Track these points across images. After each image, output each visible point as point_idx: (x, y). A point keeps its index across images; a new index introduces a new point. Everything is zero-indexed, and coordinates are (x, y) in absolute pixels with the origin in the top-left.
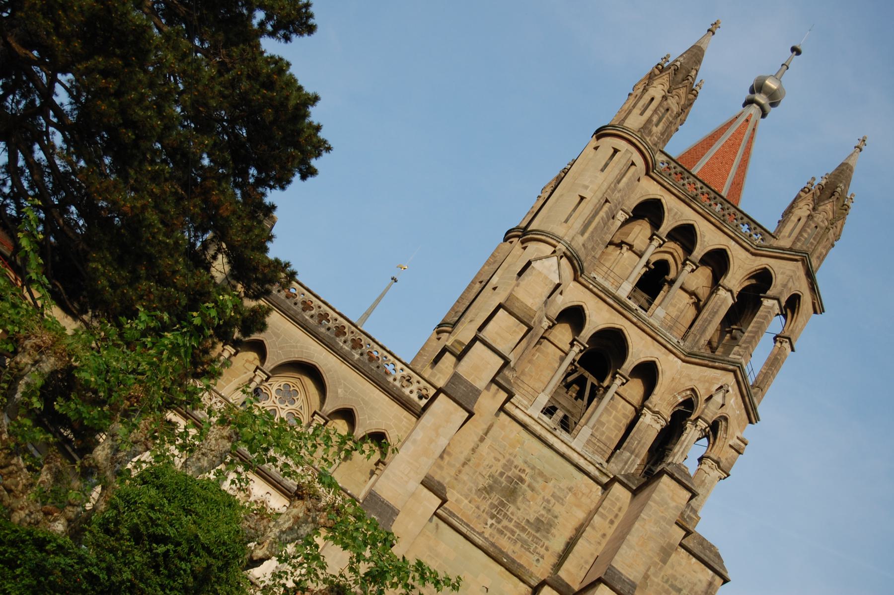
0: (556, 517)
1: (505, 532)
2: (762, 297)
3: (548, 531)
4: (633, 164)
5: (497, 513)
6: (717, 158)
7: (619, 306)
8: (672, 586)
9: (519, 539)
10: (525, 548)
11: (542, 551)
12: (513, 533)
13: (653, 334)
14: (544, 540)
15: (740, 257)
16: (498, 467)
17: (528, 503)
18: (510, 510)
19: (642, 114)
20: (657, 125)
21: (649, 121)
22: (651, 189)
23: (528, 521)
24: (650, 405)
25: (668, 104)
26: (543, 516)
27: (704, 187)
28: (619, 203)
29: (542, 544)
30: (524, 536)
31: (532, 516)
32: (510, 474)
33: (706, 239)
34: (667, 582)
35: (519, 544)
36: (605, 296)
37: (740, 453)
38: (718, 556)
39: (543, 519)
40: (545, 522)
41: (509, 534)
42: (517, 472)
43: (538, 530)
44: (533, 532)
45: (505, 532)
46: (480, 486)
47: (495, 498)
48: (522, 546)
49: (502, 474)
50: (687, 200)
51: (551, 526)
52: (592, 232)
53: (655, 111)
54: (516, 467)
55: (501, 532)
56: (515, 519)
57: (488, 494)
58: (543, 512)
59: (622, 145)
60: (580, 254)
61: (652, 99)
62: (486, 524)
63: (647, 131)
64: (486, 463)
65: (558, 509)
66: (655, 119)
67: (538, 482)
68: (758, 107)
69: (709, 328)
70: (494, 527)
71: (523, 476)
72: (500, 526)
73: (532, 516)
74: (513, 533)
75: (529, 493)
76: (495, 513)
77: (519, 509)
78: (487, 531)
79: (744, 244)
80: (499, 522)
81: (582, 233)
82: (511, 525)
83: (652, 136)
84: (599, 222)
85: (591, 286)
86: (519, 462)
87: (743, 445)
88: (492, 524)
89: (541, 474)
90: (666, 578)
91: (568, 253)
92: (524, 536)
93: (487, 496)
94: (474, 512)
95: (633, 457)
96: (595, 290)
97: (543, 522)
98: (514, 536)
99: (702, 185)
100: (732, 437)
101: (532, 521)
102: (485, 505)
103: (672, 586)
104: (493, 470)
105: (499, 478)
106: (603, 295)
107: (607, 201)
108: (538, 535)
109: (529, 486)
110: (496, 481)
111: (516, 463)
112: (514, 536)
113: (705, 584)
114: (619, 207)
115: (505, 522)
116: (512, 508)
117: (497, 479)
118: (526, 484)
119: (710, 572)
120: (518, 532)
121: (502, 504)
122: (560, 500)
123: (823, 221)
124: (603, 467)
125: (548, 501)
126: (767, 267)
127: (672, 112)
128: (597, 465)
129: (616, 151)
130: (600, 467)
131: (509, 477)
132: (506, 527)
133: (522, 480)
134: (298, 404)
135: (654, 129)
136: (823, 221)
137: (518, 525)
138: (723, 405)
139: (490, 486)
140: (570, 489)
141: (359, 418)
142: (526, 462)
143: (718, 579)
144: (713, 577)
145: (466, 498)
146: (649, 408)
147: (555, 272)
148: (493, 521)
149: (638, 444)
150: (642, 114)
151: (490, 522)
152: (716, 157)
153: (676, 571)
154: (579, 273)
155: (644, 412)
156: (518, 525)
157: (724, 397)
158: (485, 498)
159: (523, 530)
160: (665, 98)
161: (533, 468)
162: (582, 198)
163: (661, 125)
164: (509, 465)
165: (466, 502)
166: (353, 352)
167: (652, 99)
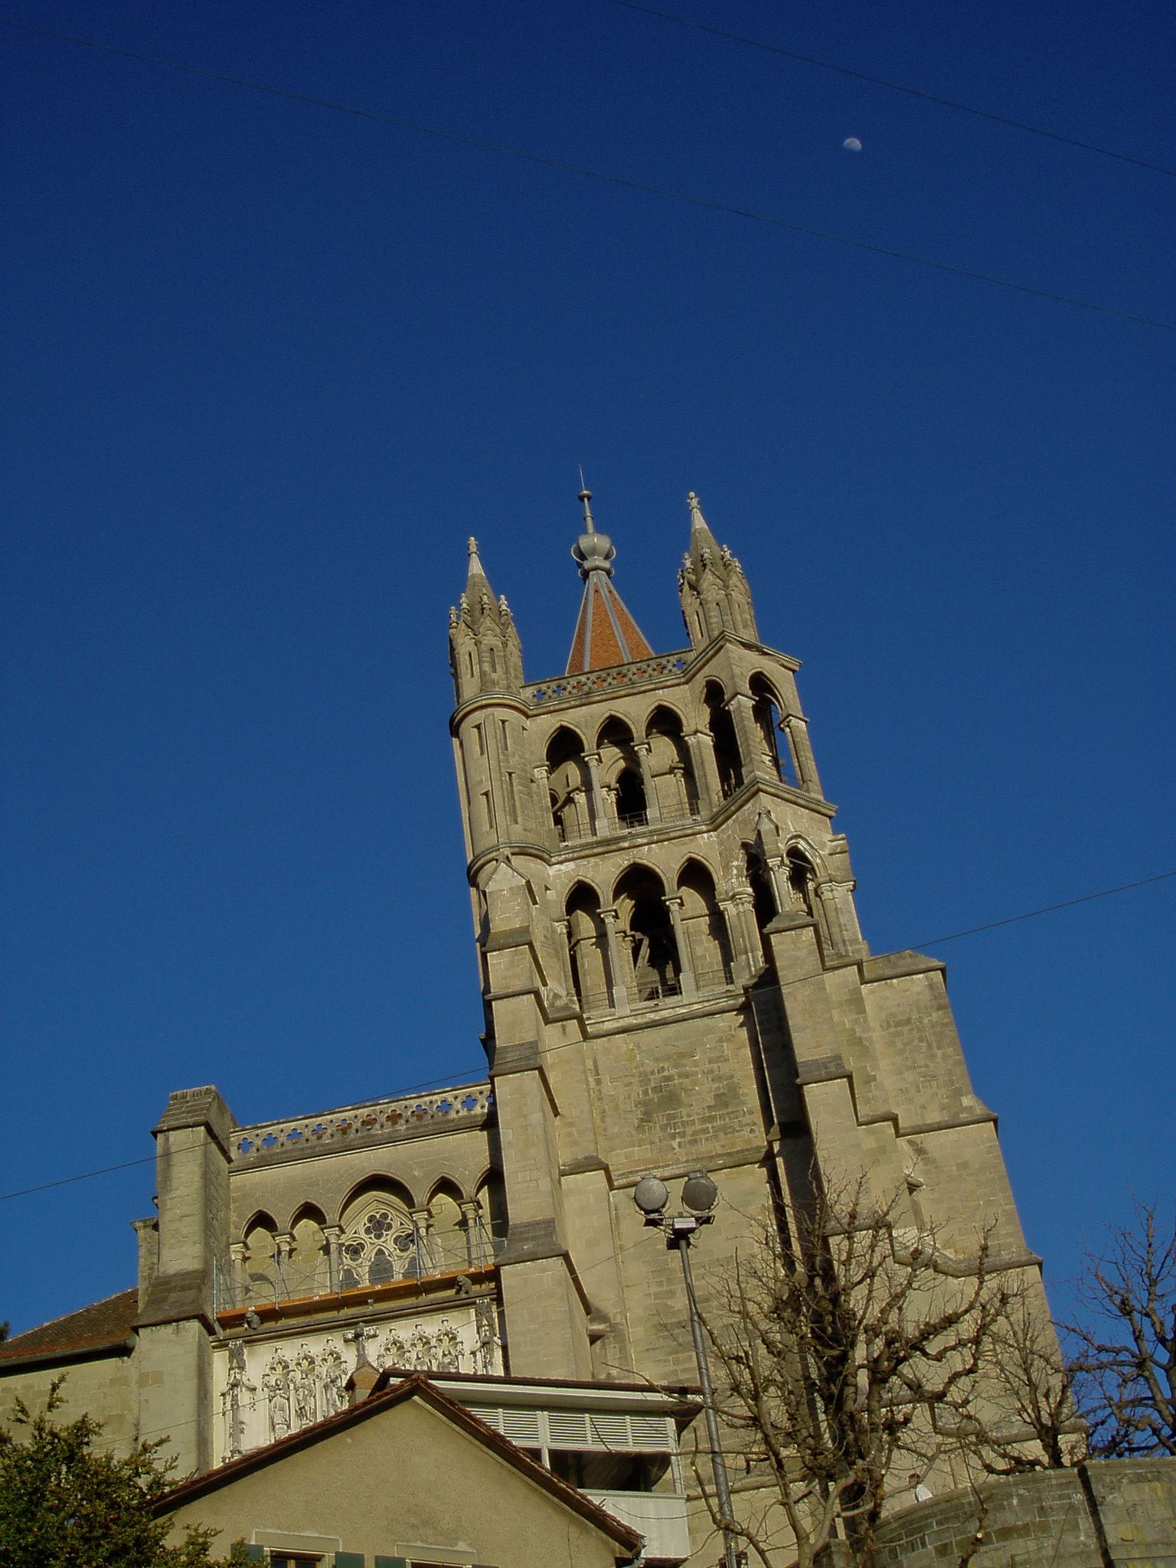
0: (732, 1076)
2: (724, 706)
3: (736, 1096)
4: (503, 722)
5: (675, 1129)
6: (597, 646)
8: (898, 1024)
9: (716, 1130)
11: (747, 1119)
12: (705, 1131)
14: (740, 1109)
16: (637, 1090)
17: (694, 1092)
18: (684, 1113)
21: (483, 674)
22: (546, 726)
24: (722, 897)
25: (485, 645)
26: (718, 1088)
28: (525, 765)
29: (742, 1112)
31: (709, 1099)
32: (653, 1085)
33: (633, 715)
34: (889, 1026)
39: (722, 1091)
40: (726, 1092)
41: (703, 1137)
43: (726, 1105)
47: (660, 1118)
48: (725, 1134)
49: (646, 1093)
50: (584, 701)
51: (735, 1089)
53: (480, 662)
54: (652, 1073)
55: (694, 1142)
57: (650, 1122)
58: (716, 1085)
59: (478, 717)
60: (530, 841)
62: (674, 1149)
63: (489, 684)
64: (621, 1098)
65: (725, 1069)
66: (487, 667)
67: (685, 1065)
68: (595, 572)
69: (709, 780)
70: (683, 1144)
71: (666, 1073)
73: (709, 1099)
74: (705, 1131)
76: (673, 1131)
77: (692, 1105)
79: (669, 683)
80: (683, 1135)
81: (516, 822)
82: (698, 1127)
83: (498, 684)
84: (520, 797)
86: (650, 1065)
89: (681, 1055)
90: (885, 1025)
93: (651, 1124)
95: (750, 954)
97: (724, 1094)
98: (709, 1133)
99: (585, 676)
101: (712, 1103)
102: (658, 1133)
103: (898, 1024)
104: (634, 1095)
105: (647, 1098)
106: (587, 852)
107: (510, 774)
109: (680, 1076)
110: (645, 1104)
111: (649, 1070)
112: (709, 1133)
114: (528, 768)
115: (689, 1130)
116: (684, 1111)
117: (645, 1101)
121: (670, 1117)
122: (722, 1059)
123: (718, 594)
124: (732, 991)
125: (711, 1071)
126: (707, 678)
127: (497, 646)
129: (478, 727)
130: (730, 994)
131: (654, 1089)
132: (695, 1133)
133: (668, 1079)
134: (396, 1224)
135: (494, 676)
136: (718, 594)
137: (704, 1120)
138: (777, 827)
139: (645, 1113)
140: (721, 1040)
141: (455, 1178)
142: (657, 1060)
145: (634, 1146)
146: (724, 900)
147: (513, 876)
148: (678, 1140)
149: (744, 940)
151: (675, 1144)
152: (595, 645)
153: (887, 1008)
154: (547, 857)
156: (704, 1120)
157: (771, 820)
158: (650, 1129)
159: (712, 1119)
161: (669, 1058)
162: (486, 794)
164: (644, 1078)
166: (397, 1127)
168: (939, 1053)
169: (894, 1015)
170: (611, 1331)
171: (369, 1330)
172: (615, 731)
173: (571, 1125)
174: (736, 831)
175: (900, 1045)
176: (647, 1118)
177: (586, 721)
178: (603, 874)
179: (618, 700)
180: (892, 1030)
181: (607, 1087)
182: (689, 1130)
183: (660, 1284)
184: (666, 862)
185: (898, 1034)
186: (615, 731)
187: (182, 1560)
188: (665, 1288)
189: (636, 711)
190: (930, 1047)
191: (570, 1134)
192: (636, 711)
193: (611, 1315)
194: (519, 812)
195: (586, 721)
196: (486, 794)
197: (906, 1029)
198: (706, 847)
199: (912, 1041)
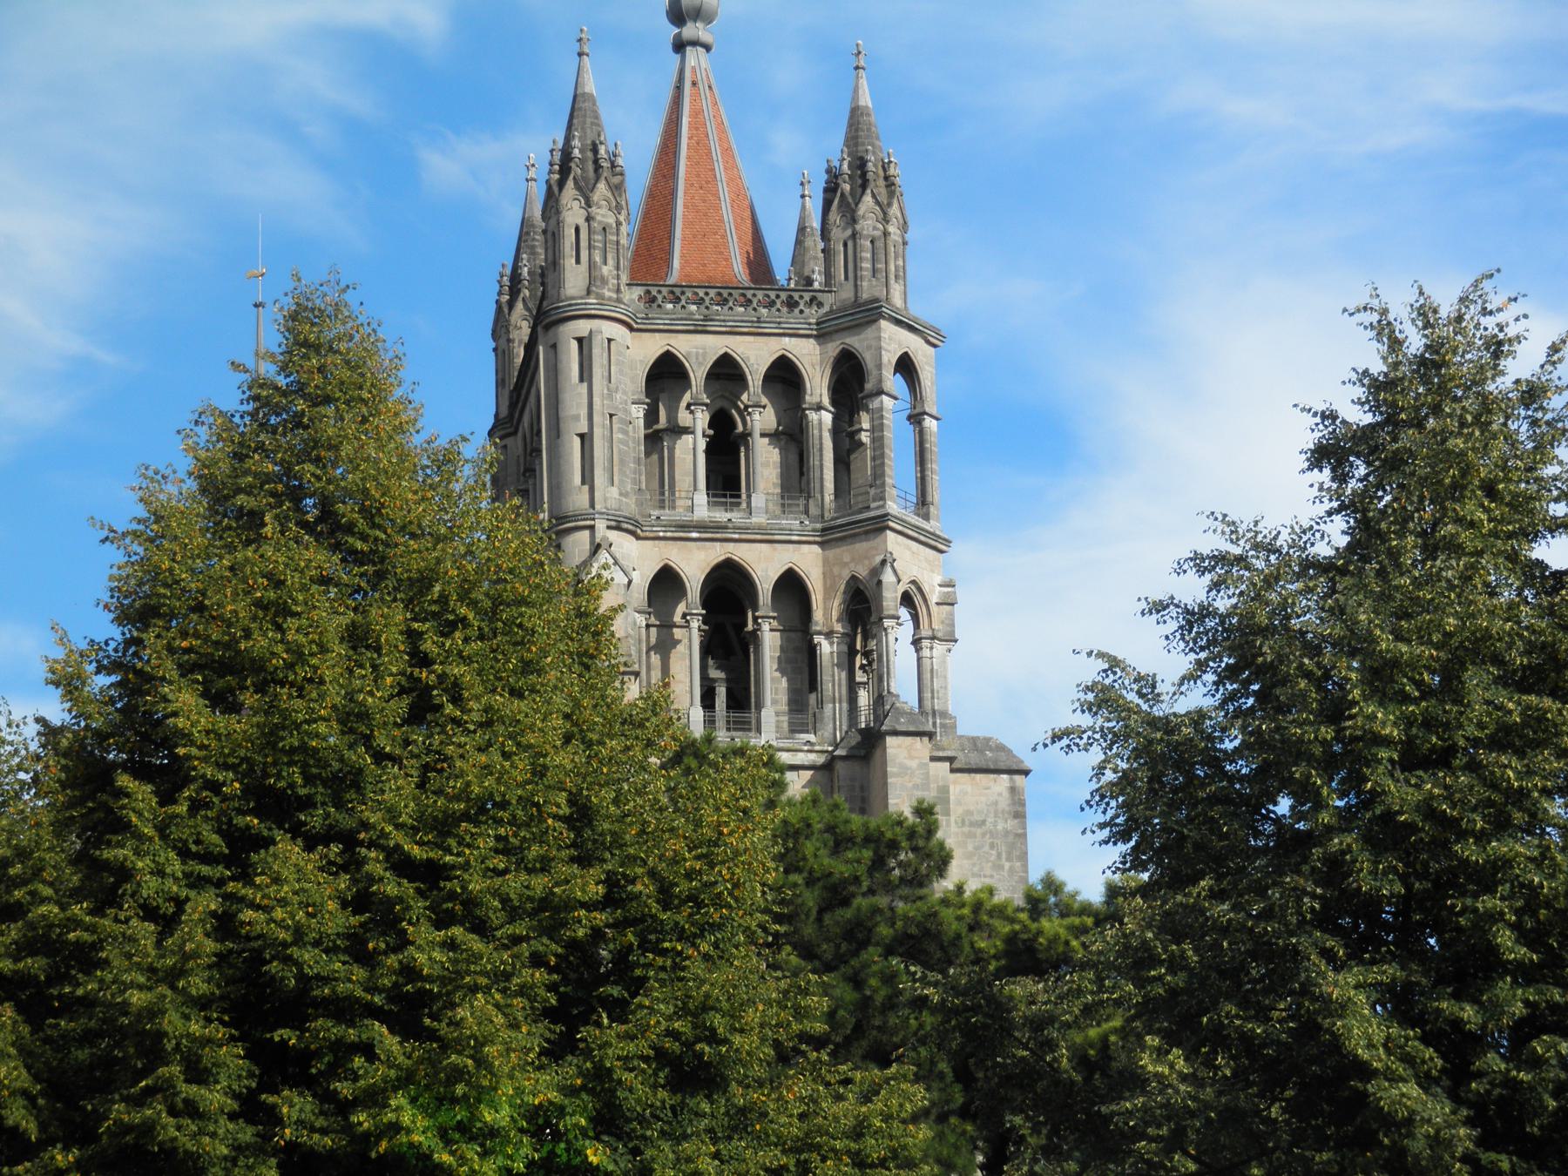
4: (610, 340)
7: (710, 531)
8: (972, 824)
13: (767, 537)
15: (804, 352)
19: (578, 261)
20: (605, 263)
21: (591, 265)
22: (648, 349)
25: (600, 222)
27: (708, 290)
34: (963, 822)
36: (684, 530)
37: (952, 604)
38: (1001, 748)
52: (620, 470)
59: (582, 327)
61: (577, 230)
63: (598, 283)
66: (598, 258)
79: (802, 332)
85: (661, 534)
87: (950, 589)
90: (960, 821)
91: (613, 523)
96: (669, 534)
100: (933, 591)
103: (972, 824)
107: (611, 416)
113: (1006, 794)
119: (1005, 776)
127: (611, 227)
128: (806, 748)
129: (580, 340)
143: (1017, 778)
144: (1011, 779)
146: (819, 633)
150: (578, 261)
152: (689, 185)
155: (816, 641)
160: (589, 219)
162: (582, 436)
163: (611, 262)
167: (577, 230)
168: (1007, 865)
169: (970, 813)
172: (727, 372)
174: (854, 559)
175: (970, 848)
177: (698, 352)
178: (695, 563)
179: (738, 337)
180: (966, 829)
184: (765, 566)
185: (971, 835)
186: (727, 372)
189: (756, 355)
190: (999, 856)
192: (756, 355)
194: (616, 469)
195: (698, 352)
196: (582, 436)
197: (979, 831)
198: (809, 562)
199: (983, 846)
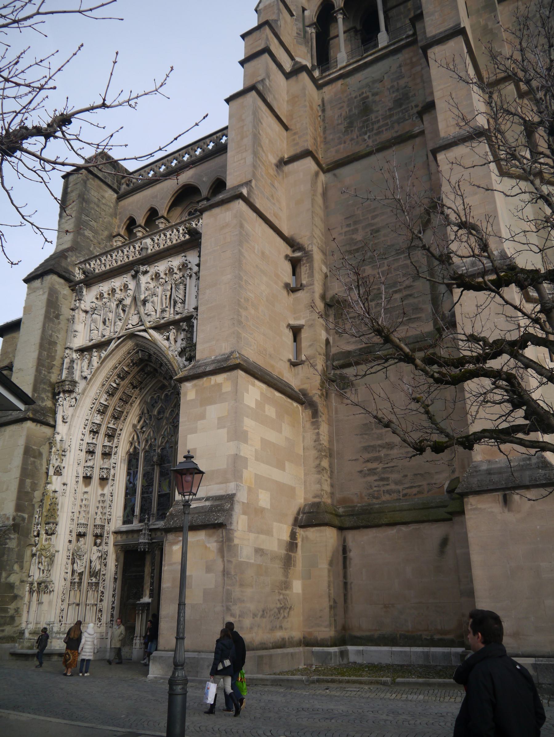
1: (381, 130)
10: (402, 122)
12: (387, 124)
23: (390, 109)
29: (410, 108)
30: (395, 118)
31: (390, 104)
35: (396, 125)
41: (384, 129)
42: (359, 98)
43: (401, 105)
44: (399, 109)
45: (381, 130)
46: (343, 130)
54: (356, 97)
55: (378, 133)
56: (380, 118)
71: (364, 95)
72: (375, 132)
75: (377, 98)
78: (370, 143)
82: (381, 123)
88: (369, 137)
92: (395, 118)
94: (352, 144)
97: (400, 99)
104: (344, 114)
108: (403, 107)
109: (373, 95)
111: (354, 96)
115: (376, 126)
116: (373, 116)
118: (370, 96)
120: (388, 121)
132: (379, 127)
140: (400, 66)
148: (368, 134)
151: (366, 137)
158: (352, 131)
159: (391, 116)
165: (342, 146)
170: (305, 256)
171: (143, 268)
173: (295, 134)
176: (350, 126)
181: (329, 113)
182: (376, 126)
183: (348, 225)
187: (253, 405)
188: (352, 228)
191: (294, 140)
193: (306, 246)
